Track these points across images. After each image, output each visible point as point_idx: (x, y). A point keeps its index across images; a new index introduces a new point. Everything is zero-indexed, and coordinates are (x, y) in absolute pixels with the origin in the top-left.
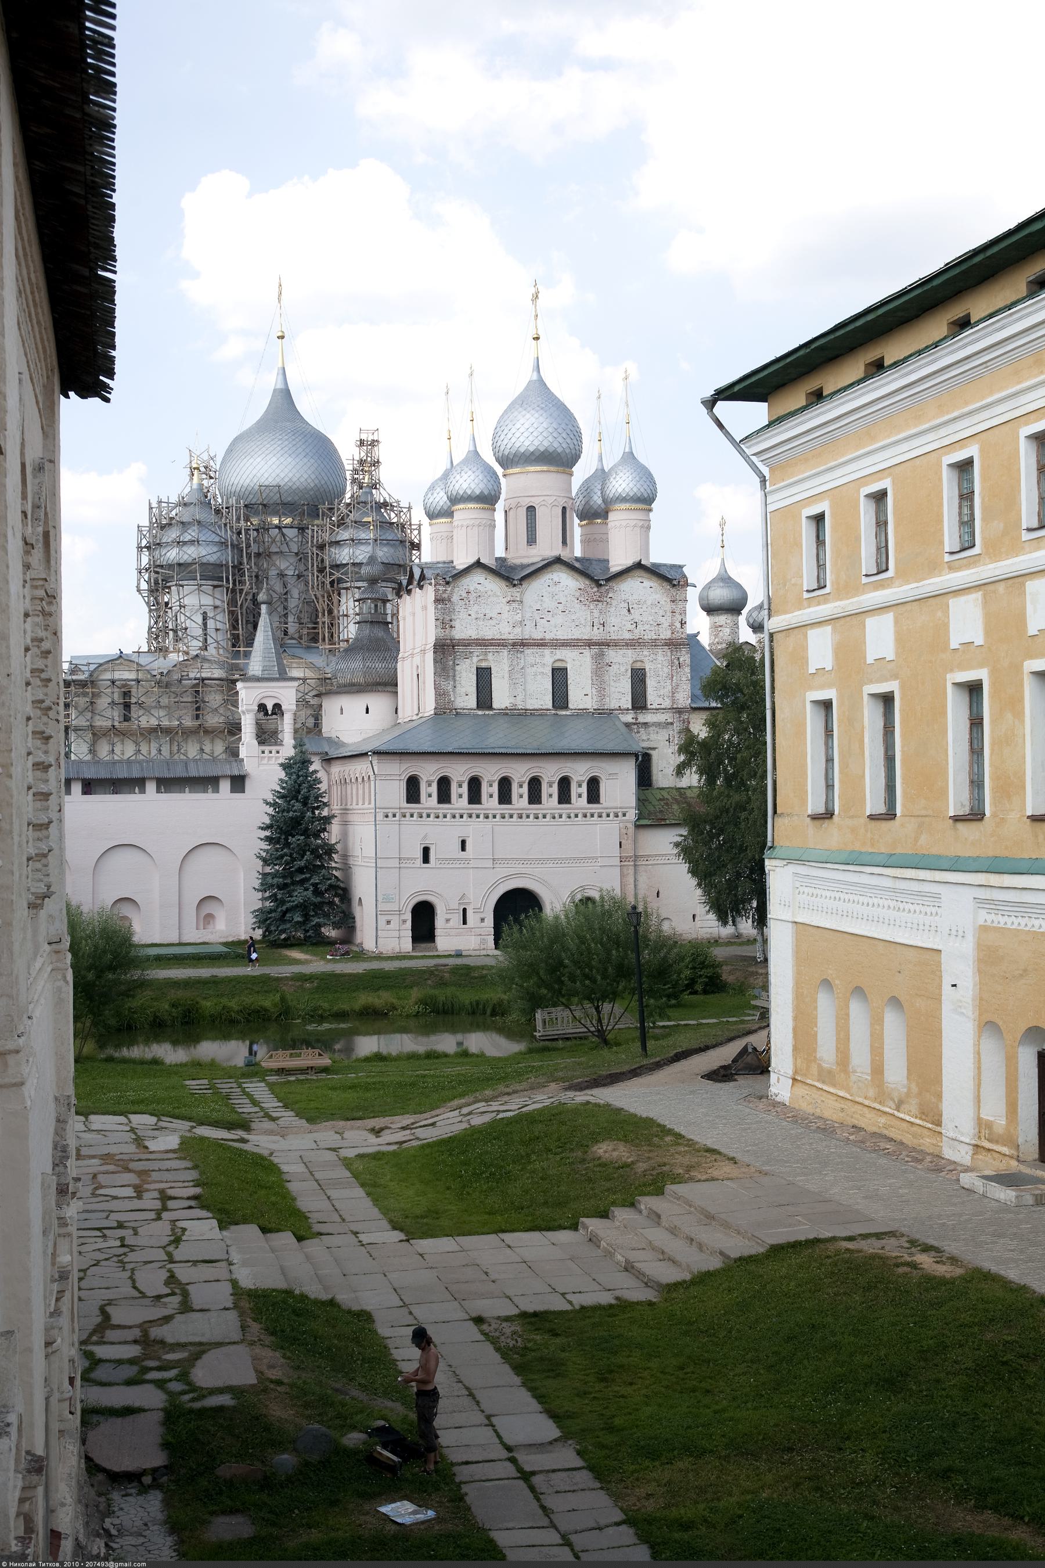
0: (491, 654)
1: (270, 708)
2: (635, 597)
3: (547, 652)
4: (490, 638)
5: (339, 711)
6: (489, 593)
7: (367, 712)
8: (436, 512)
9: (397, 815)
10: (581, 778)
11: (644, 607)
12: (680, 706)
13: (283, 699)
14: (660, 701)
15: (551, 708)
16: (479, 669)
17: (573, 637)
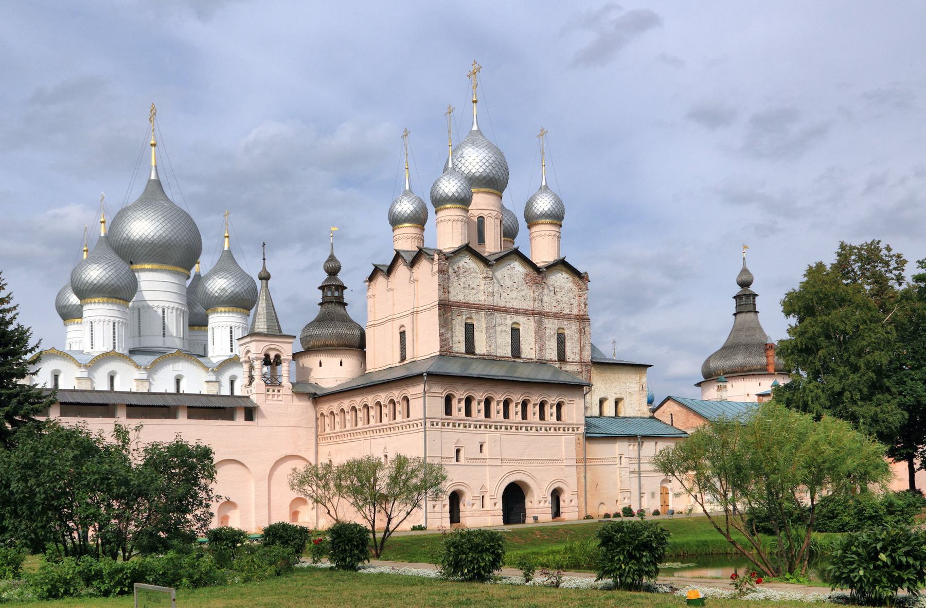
0: (474, 314)
1: (272, 356)
2: (558, 283)
3: (508, 316)
4: (472, 302)
5: (318, 364)
6: (472, 270)
7: (341, 365)
8: (403, 218)
9: (440, 424)
10: (553, 402)
11: (563, 291)
12: (585, 361)
13: (282, 351)
14: (573, 357)
15: (510, 355)
16: (466, 324)
17: (523, 308)
